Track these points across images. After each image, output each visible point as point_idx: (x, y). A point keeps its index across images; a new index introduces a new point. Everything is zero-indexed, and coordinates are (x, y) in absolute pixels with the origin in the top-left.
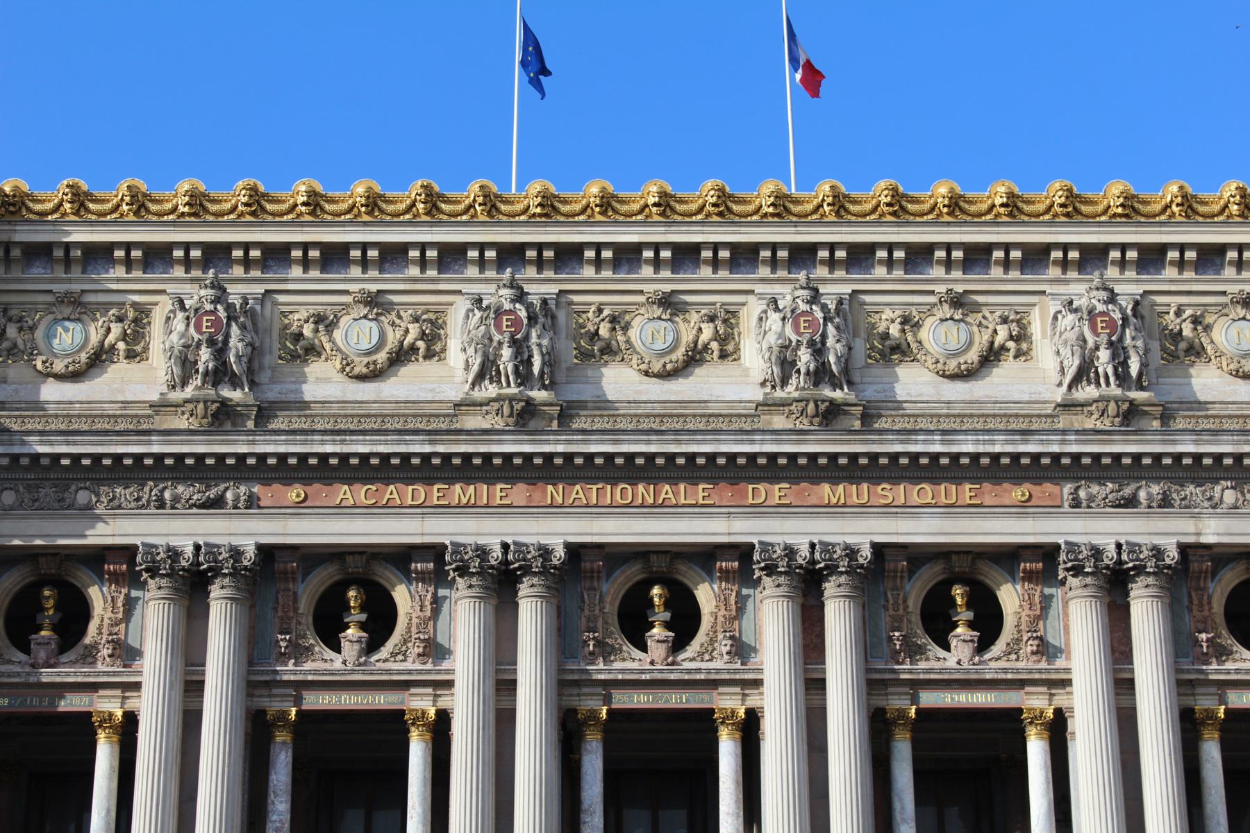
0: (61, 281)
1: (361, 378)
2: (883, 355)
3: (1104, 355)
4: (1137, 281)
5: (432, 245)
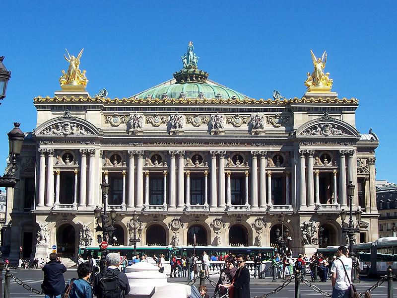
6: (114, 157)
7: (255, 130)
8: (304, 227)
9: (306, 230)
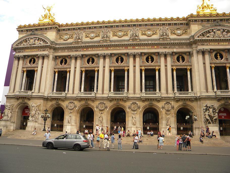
0: (66, 32)
1: (92, 39)
2: (142, 35)
3: (164, 33)
4: (168, 27)
5: (99, 26)
6: (64, 60)
7: (162, 37)
8: (207, 109)
9: (208, 111)
